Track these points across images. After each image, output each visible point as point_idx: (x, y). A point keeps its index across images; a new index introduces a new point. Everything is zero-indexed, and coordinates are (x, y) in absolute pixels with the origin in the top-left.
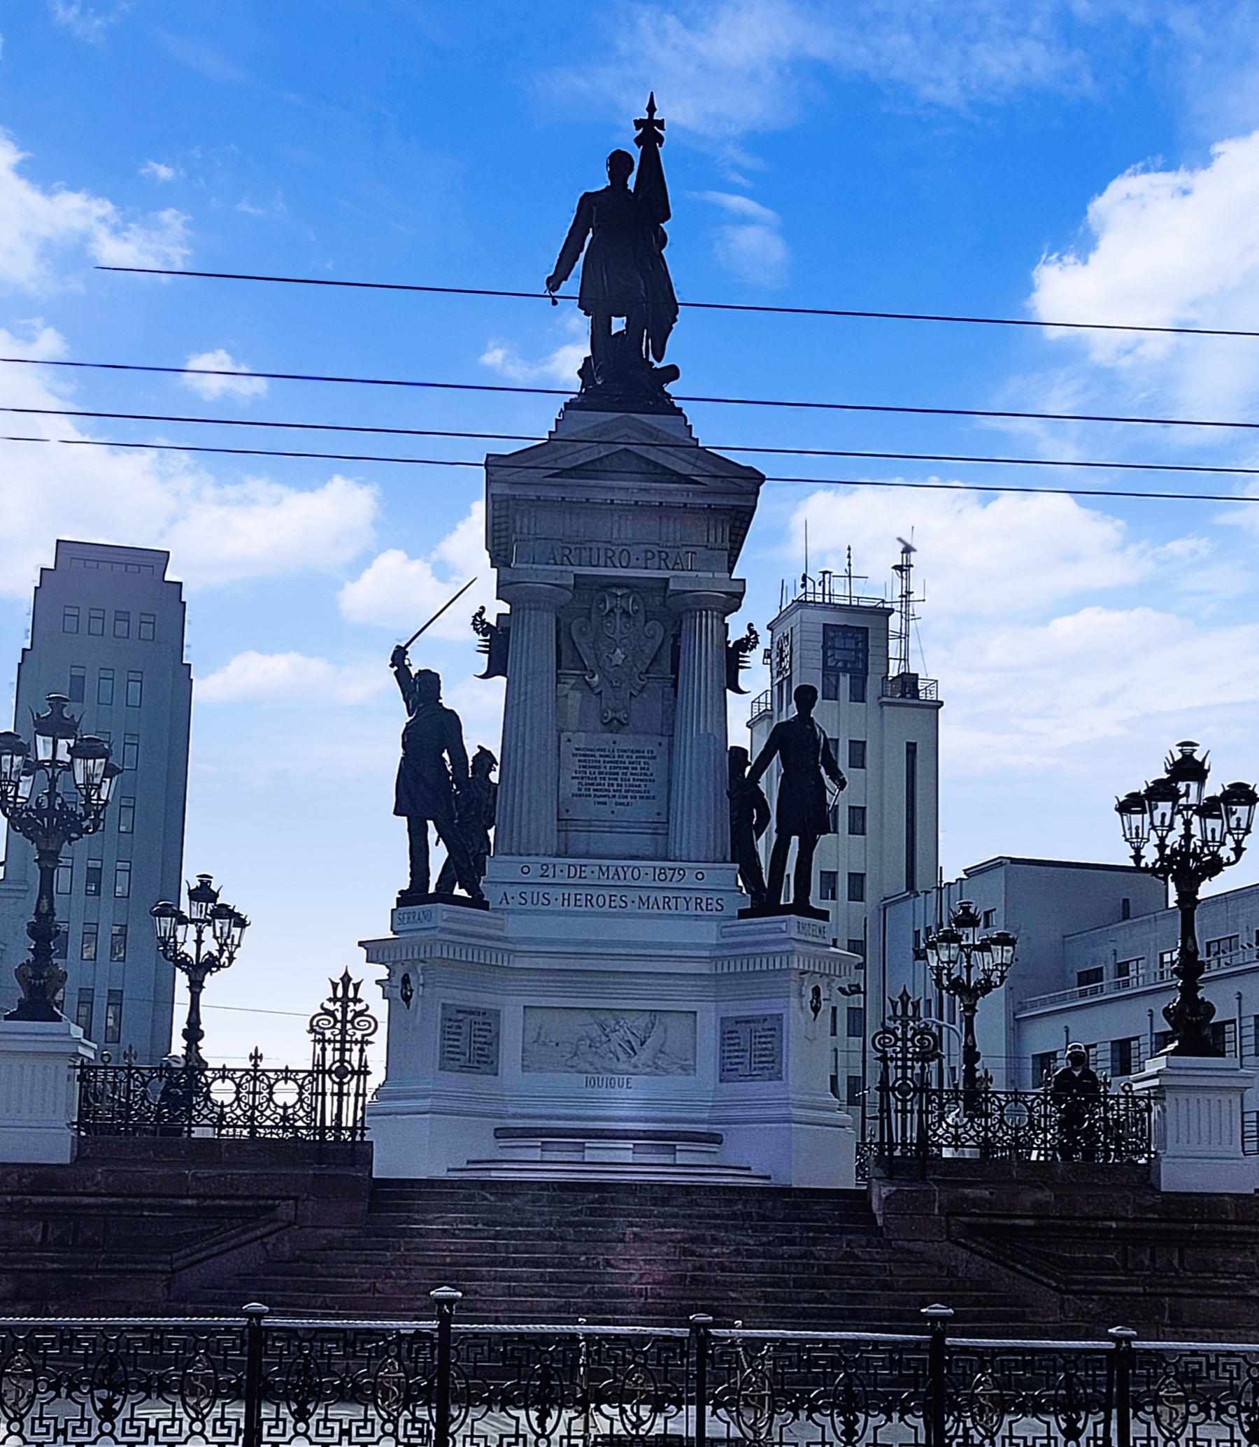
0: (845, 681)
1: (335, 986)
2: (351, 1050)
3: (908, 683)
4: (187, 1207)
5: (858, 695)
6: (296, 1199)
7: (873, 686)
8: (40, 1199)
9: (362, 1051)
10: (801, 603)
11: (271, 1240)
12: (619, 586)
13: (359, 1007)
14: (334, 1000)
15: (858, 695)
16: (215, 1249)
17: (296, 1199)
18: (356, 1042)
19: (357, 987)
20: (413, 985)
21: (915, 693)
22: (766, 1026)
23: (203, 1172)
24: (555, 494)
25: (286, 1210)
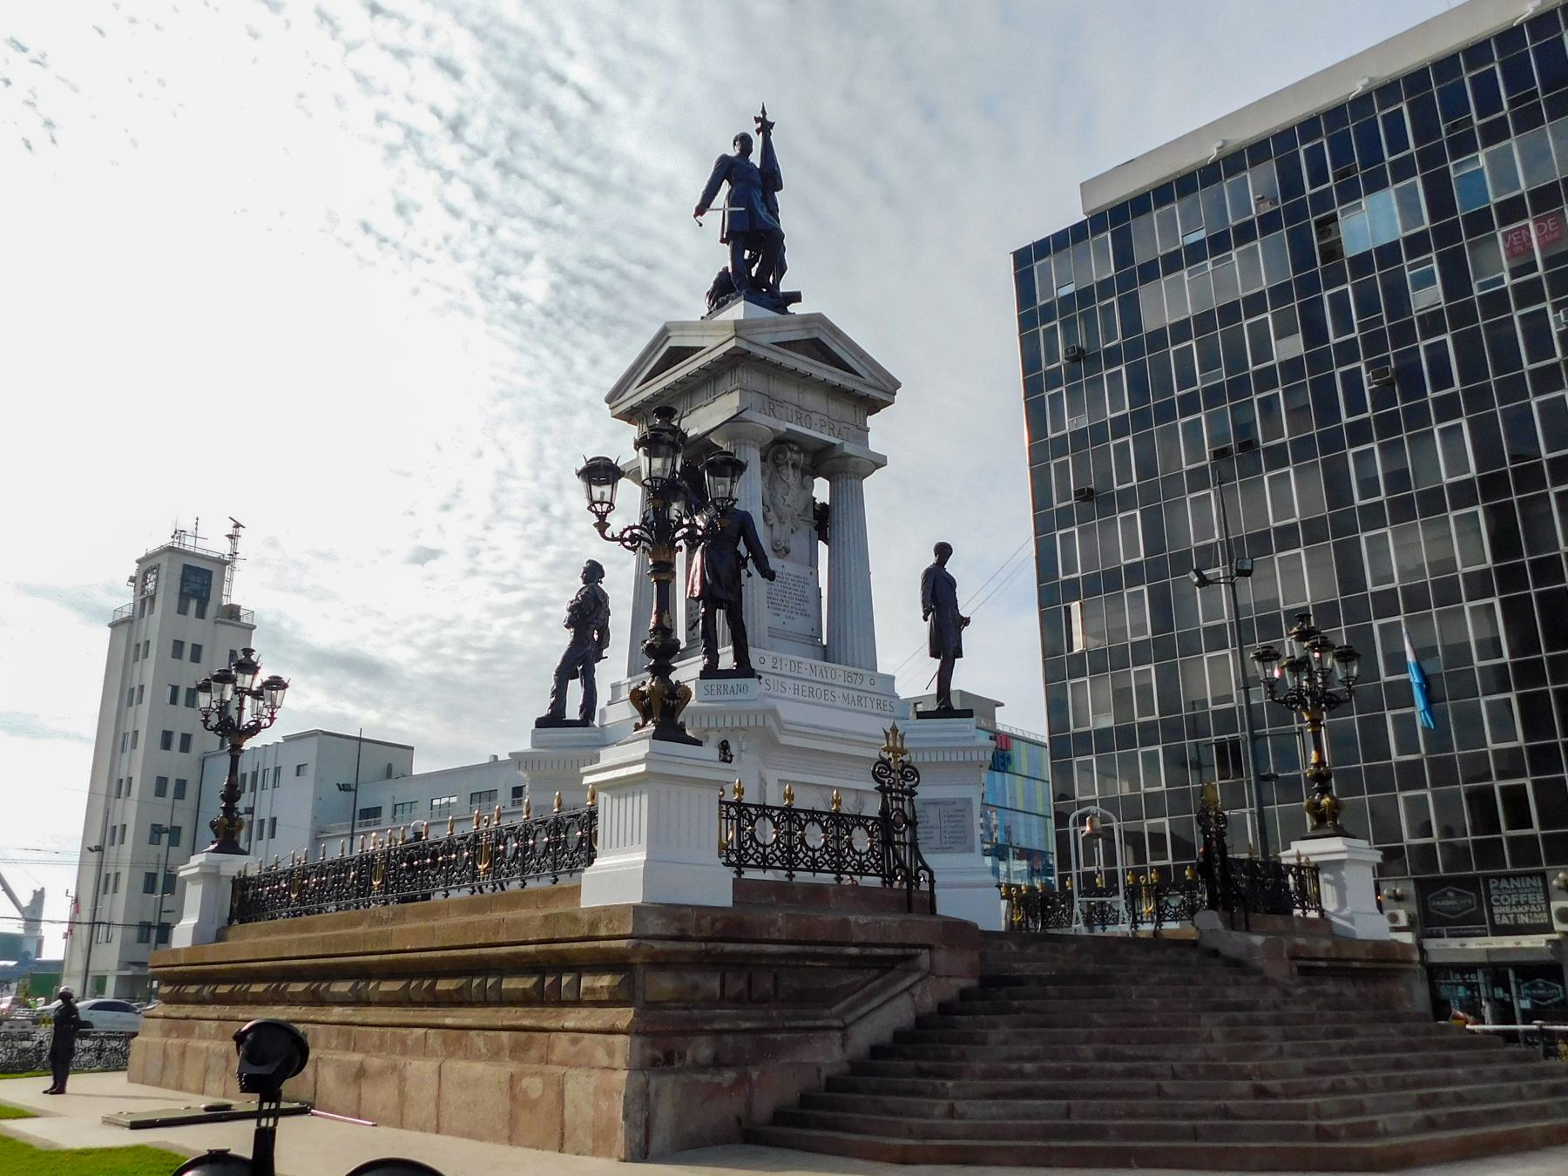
0: (193, 605)
1: (887, 735)
2: (903, 800)
3: (233, 612)
4: (850, 956)
5: (201, 614)
6: (930, 947)
7: (211, 610)
8: (730, 947)
9: (911, 801)
10: (170, 549)
11: (917, 990)
12: (794, 443)
13: (906, 758)
14: (888, 750)
15: (201, 614)
16: (876, 1002)
17: (930, 947)
18: (904, 792)
19: (902, 738)
20: (733, 750)
21: (238, 618)
22: (955, 807)
23: (863, 920)
24: (775, 358)
25: (924, 958)
